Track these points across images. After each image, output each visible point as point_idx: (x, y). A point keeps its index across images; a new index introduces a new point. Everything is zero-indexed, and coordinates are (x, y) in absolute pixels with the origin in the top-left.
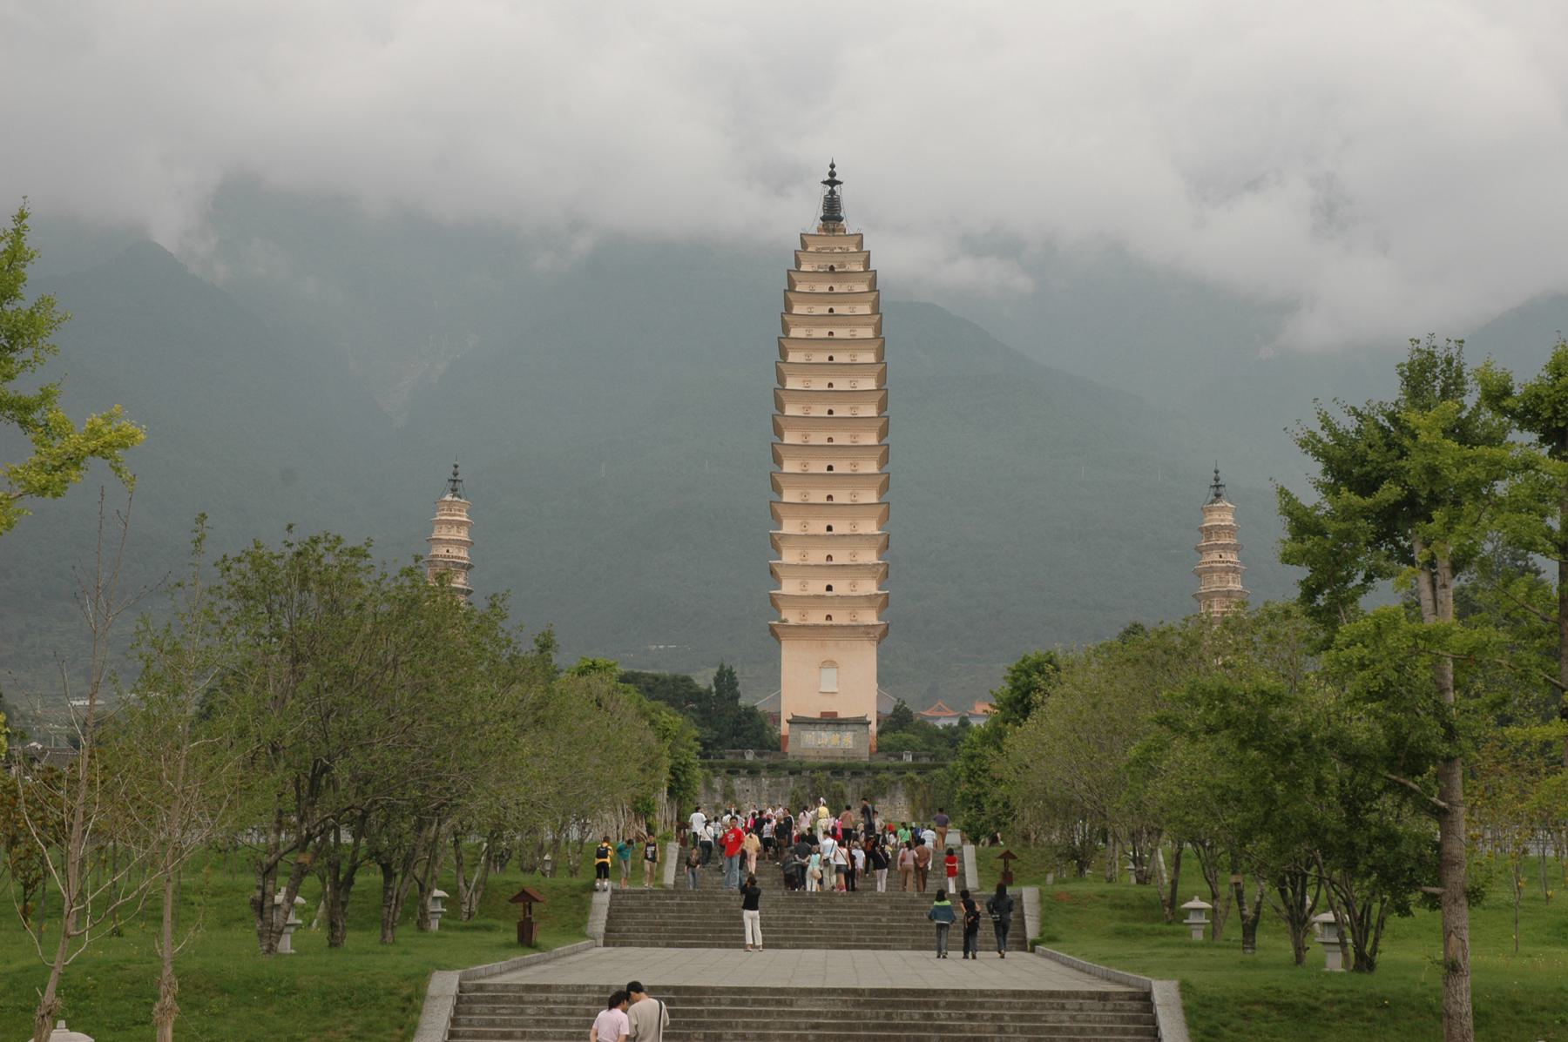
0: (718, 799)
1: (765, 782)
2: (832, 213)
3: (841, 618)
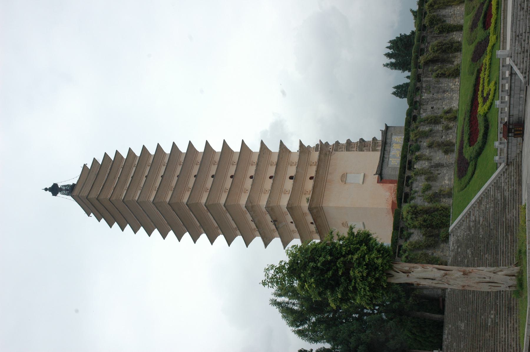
0: (439, 128)
1: (425, 96)
2: (70, 190)
3: (312, 171)
